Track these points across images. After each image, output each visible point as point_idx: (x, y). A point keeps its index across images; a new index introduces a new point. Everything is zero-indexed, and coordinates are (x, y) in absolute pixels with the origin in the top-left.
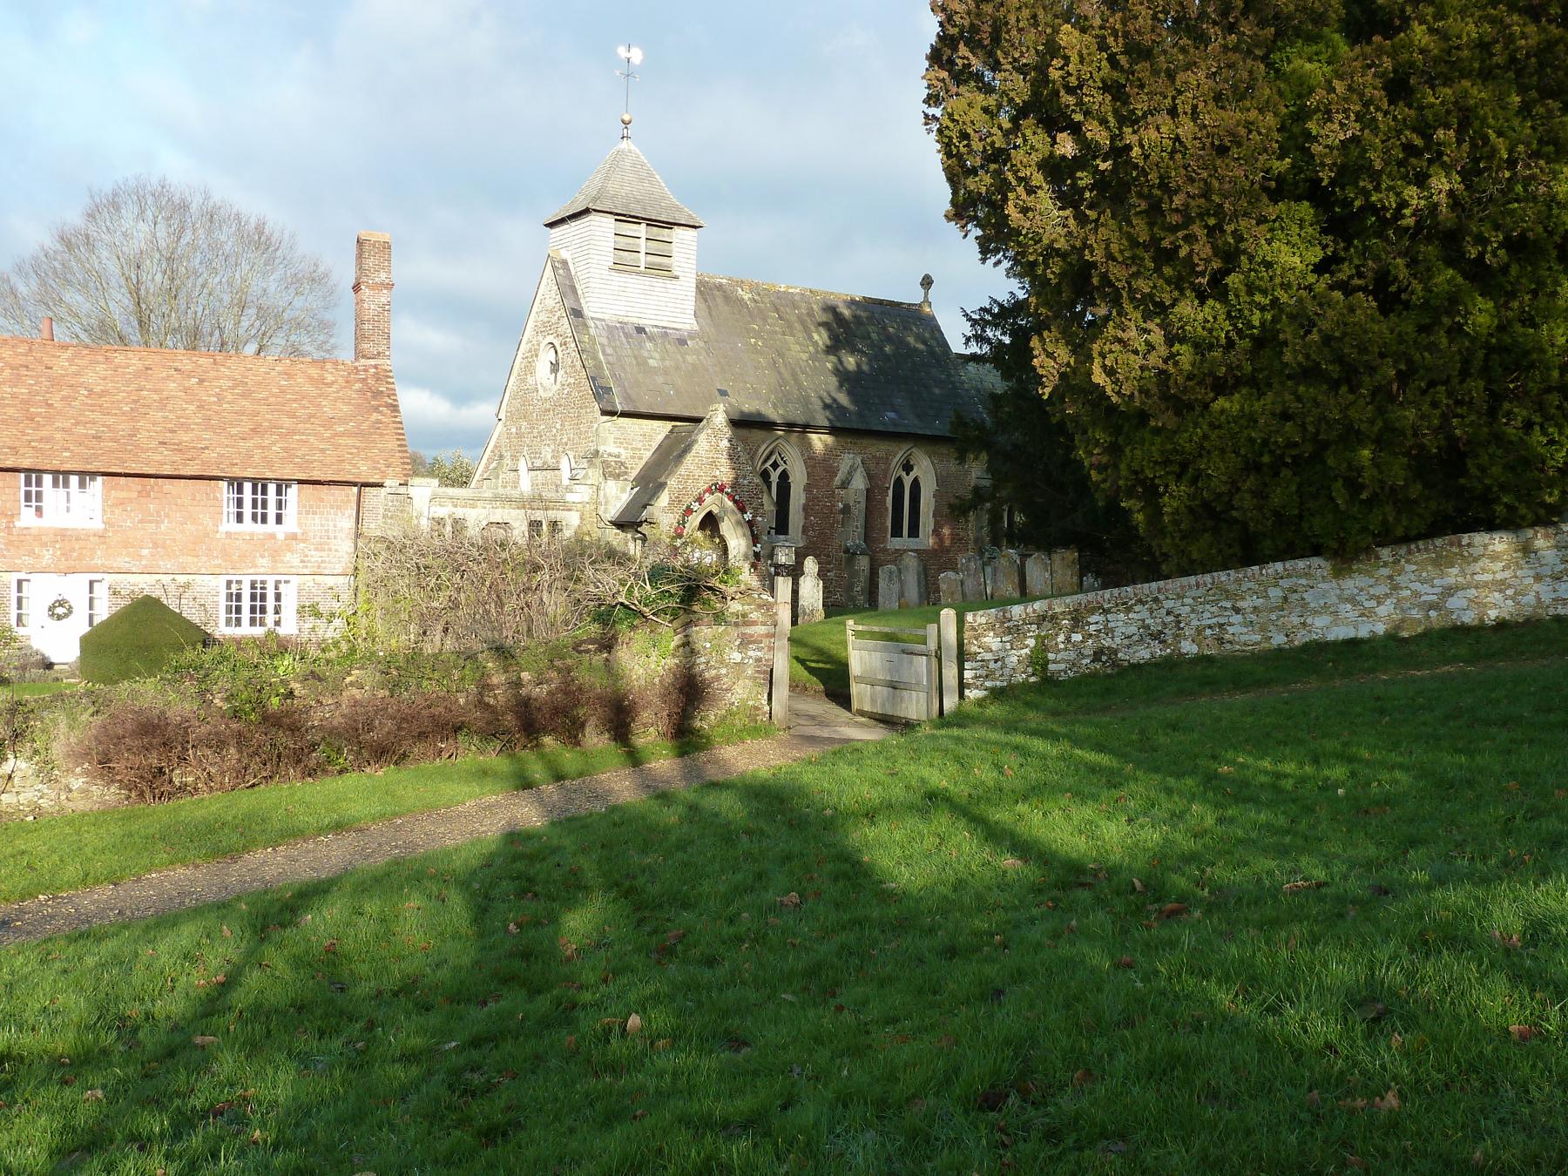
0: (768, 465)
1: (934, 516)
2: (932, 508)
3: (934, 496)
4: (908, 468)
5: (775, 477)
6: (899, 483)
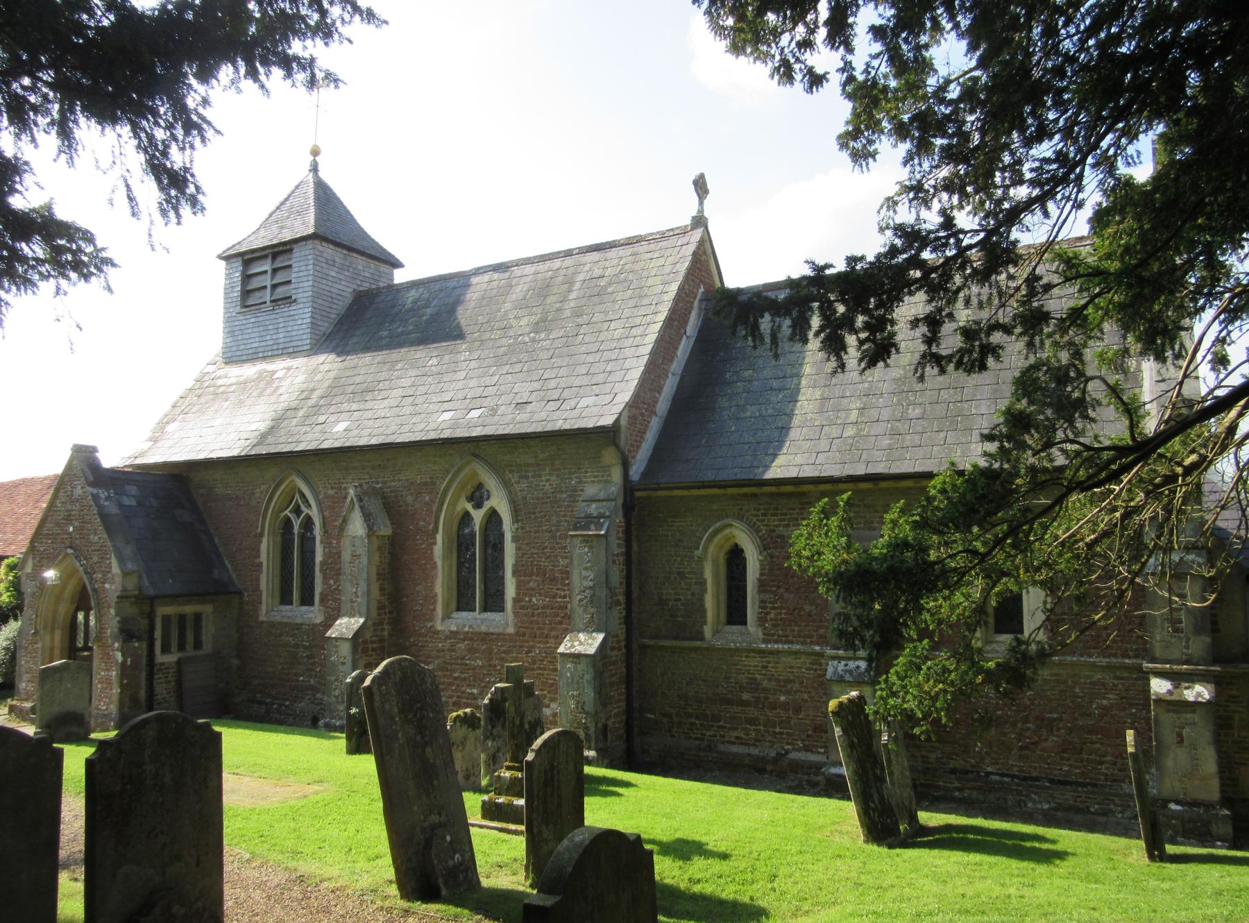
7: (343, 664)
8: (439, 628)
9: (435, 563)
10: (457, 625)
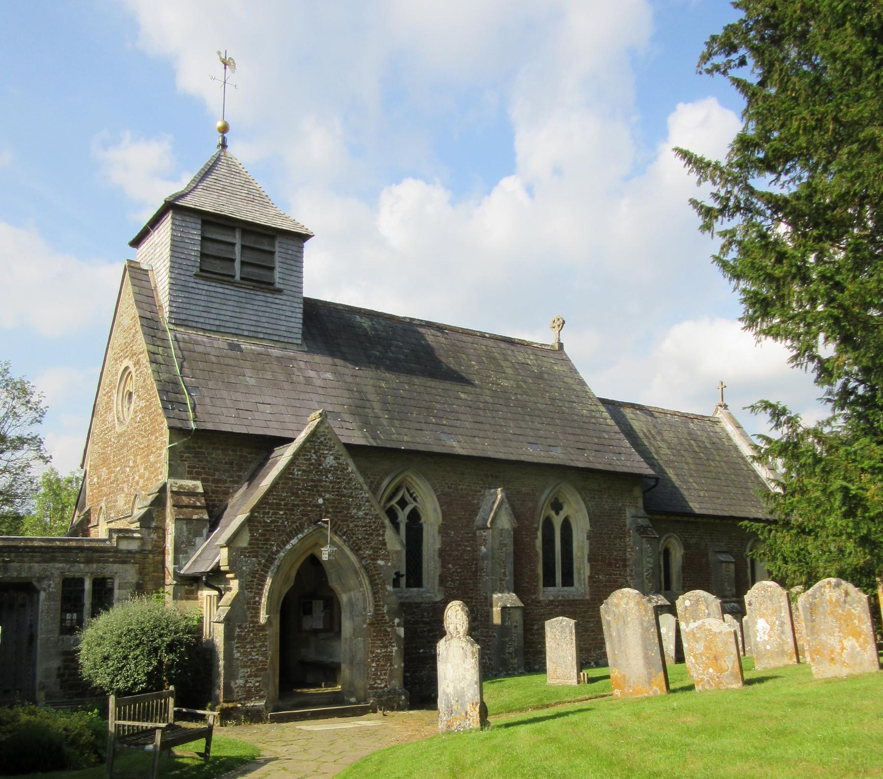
0: (393, 502)
1: (590, 560)
2: (586, 552)
3: (589, 538)
4: (557, 507)
5: (403, 516)
6: (548, 524)
7: (516, 627)
8: (541, 599)
9: (537, 552)
10: (553, 596)
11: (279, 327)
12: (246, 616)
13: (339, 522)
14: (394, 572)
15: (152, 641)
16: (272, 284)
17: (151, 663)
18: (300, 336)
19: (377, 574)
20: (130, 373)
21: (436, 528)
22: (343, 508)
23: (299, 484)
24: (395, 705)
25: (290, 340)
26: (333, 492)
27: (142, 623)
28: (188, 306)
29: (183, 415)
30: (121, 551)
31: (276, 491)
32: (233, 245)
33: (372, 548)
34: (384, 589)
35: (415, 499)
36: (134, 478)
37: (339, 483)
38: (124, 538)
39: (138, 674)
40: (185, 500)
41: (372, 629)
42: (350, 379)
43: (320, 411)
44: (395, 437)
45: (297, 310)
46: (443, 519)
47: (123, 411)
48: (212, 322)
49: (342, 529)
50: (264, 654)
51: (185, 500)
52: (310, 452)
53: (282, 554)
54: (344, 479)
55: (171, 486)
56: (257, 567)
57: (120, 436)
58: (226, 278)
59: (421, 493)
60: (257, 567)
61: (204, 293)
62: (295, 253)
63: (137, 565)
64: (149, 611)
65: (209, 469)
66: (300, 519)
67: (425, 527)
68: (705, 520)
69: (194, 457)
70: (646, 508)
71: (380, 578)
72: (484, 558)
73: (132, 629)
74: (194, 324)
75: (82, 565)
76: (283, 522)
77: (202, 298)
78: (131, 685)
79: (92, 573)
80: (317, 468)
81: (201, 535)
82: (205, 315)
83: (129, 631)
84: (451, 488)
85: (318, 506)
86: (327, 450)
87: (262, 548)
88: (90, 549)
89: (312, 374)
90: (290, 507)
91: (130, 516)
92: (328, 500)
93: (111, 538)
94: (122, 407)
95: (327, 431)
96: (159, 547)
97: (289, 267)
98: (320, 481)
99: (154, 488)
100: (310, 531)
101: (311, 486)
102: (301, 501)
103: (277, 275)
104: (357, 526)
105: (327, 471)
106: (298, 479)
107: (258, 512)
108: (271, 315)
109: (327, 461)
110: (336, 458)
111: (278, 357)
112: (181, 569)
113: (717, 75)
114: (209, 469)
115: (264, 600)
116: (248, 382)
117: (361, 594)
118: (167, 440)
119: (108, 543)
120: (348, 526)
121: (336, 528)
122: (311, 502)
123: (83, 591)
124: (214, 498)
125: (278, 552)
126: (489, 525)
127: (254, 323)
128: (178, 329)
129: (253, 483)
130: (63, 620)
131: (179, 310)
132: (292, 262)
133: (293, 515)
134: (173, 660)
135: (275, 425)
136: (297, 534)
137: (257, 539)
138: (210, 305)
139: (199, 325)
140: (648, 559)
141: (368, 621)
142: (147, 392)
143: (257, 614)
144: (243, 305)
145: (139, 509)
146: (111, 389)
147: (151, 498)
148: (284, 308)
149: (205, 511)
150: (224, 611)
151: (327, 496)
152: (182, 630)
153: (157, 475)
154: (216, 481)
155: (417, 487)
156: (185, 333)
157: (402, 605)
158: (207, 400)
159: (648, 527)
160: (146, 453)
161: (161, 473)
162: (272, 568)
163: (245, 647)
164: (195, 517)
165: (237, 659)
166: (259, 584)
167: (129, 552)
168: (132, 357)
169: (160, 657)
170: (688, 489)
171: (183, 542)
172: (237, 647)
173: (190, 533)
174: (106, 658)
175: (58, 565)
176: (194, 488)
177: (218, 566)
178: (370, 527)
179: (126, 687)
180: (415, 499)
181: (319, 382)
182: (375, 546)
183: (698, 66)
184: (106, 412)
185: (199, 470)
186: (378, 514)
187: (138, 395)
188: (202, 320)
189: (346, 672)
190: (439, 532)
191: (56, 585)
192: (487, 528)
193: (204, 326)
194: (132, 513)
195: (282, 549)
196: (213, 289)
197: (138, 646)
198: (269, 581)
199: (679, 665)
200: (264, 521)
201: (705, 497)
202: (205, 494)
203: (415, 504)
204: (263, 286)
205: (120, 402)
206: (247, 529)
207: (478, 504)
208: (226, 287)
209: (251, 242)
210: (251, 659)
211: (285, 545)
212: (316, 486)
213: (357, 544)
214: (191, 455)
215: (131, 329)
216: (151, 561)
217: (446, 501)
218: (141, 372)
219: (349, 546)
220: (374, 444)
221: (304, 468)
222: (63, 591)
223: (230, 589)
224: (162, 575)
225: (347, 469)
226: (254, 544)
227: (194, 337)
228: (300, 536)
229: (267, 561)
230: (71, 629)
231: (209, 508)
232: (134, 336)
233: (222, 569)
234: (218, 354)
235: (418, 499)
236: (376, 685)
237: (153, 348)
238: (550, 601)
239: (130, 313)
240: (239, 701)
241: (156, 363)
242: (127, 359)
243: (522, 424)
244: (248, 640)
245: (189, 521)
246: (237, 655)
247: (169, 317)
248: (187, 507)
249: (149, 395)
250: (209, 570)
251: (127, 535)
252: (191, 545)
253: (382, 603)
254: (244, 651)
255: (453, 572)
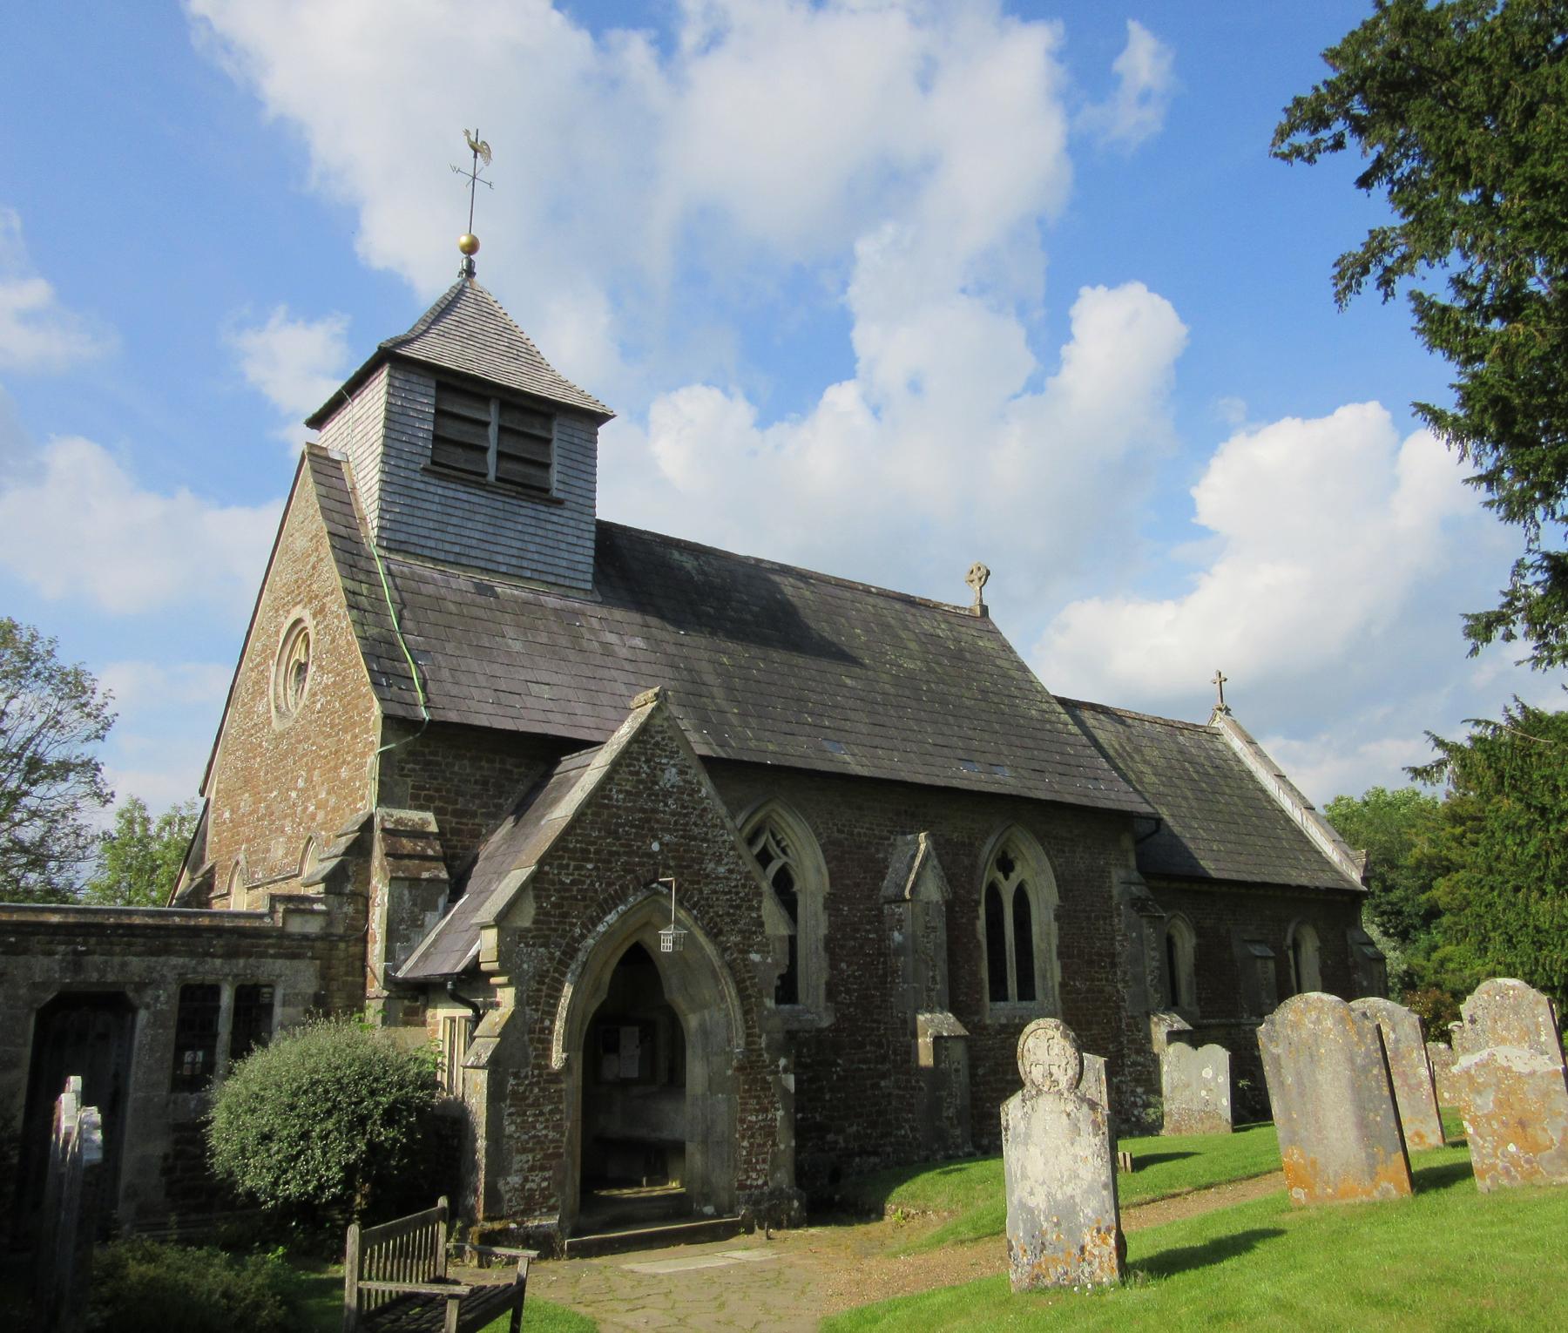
4: (1006, 866)
9: (978, 941)
11: (557, 561)
12: (526, 1056)
13: (686, 885)
14: (777, 974)
15: (356, 1104)
16: (547, 491)
17: (354, 1147)
18: (589, 577)
19: (749, 978)
20: (305, 628)
21: (820, 900)
22: (693, 860)
23: (620, 817)
24: (784, 1217)
25: (574, 584)
26: (677, 830)
27: (337, 1068)
28: (410, 520)
29: (407, 696)
30: (290, 936)
31: (581, 828)
32: (486, 424)
33: (740, 931)
34: (761, 1004)
35: (784, 851)
36: (306, 808)
37: (686, 815)
38: (297, 911)
39: (329, 1168)
40: (407, 845)
41: (742, 1078)
42: (672, 649)
43: (656, 690)
44: (753, 744)
45: (587, 535)
46: (832, 885)
47: (285, 695)
48: (447, 547)
49: (692, 897)
50: (557, 1127)
51: (407, 845)
52: (639, 760)
53: (591, 941)
54: (695, 809)
55: (382, 819)
56: (548, 965)
57: (282, 736)
58: (473, 478)
59: (794, 838)
60: (548, 965)
61: (437, 499)
62: (583, 443)
63: (318, 962)
64: (348, 1045)
65: (448, 791)
66: (620, 877)
67: (800, 898)
68: (1224, 889)
69: (422, 770)
70: (1140, 868)
71: (753, 985)
72: (900, 950)
73: (318, 1081)
74: (419, 551)
75: (218, 962)
76: (592, 884)
77: (434, 507)
78: (315, 1188)
79: (236, 976)
80: (650, 789)
81: (435, 908)
82: (438, 535)
83: (314, 1083)
84: (843, 832)
85: (652, 855)
86: (666, 757)
87: (555, 930)
88: (234, 931)
89: (611, 638)
90: (604, 855)
91: (296, 876)
92: (667, 845)
93: (272, 911)
94: (285, 689)
95: (666, 724)
96: (357, 929)
97: (575, 465)
98: (654, 811)
99: (349, 823)
100: (639, 899)
101: (640, 820)
102: (622, 845)
103: (555, 476)
104: (715, 892)
105: (667, 794)
106: (618, 808)
107: (551, 865)
108: (544, 541)
109: (667, 775)
110: (681, 772)
111: (556, 609)
112: (397, 969)
113: (1297, 161)
114: (448, 791)
115: (559, 1026)
116: (509, 647)
117: (723, 1014)
118: (376, 737)
119: (267, 920)
120: (701, 892)
121: (680, 895)
122: (639, 848)
123: (218, 1008)
124: (454, 843)
125: (583, 937)
126: (908, 896)
127: (515, 552)
128: (392, 556)
129: (525, 817)
130: (178, 1061)
131: (395, 526)
132: (580, 458)
133: (610, 870)
134: (395, 1140)
135: (558, 718)
136: (616, 906)
137: (547, 914)
138: (445, 519)
139: (427, 552)
140: (1153, 954)
141: (735, 1063)
142: (338, 659)
143: (546, 1053)
144: (499, 522)
145: (322, 860)
146: (265, 659)
147: (344, 843)
148: (565, 530)
149: (442, 865)
150: (485, 1046)
151: (667, 838)
152: (411, 1082)
153: (355, 802)
154: (456, 813)
155: (788, 830)
156: (403, 564)
157: (791, 1035)
158: (445, 674)
159: (1148, 899)
160: (332, 764)
161: (363, 798)
162: (573, 966)
163: (525, 1114)
164: (425, 875)
165: (510, 1137)
166: (549, 996)
167: (305, 937)
168: (310, 602)
169: (371, 1133)
170: (1194, 839)
171: (402, 920)
172: (510, 1115)
173: (415, 904)
174: (266, 1138)
175: (174, 960)
176: (423, 825)
177: (476, 962)
178: (737, 893)
179: (302, 1195)
180: (784, 851)
181: (623, 652)
182: (745, 928)
183: (1273, 145)
184: (253, 699)
185: (431, 793)
186: (749, 872)
187: (320, 667)
188: (431, 543)
189: (695, 1157)
190: (826, 907)
191: (169, 996)
192: (905, 900)
193: (434, 555)
194: (301, 870)
195: (589, 931)
196: (451, 493)
197: (329, 1113)
198: (568, 990)
199: (1257, 1134)
200: (560, 880)
201: (1219, 851)
202: (440, 835)
203: (784, 859)
204: (534, 493)
205: (281, 681)
206: (531, 893)
207: (885, 859)
208: (473, 491)
209: (513, 420)
210: (534, 1137)
211: (595, 925)
212: (648, 820)
213: (716, 924)
214: (417, 767)
215: (310, 555)
216: (342, 955)
217: (836, 854)
218: (326, 627)
219: (702, 928)
220: (724, 756)
221: (628, 788)
222: (181, 1009)
223: (497, 1005)
224: (360, 980)
225: (699, 791)
226: (542, 922)
227: (417, 569)
228: (621, 908)
229: (564, 953)
230: (196, 1081)
231: (448, 859)
232: (314, 568)
233: (484, 967)
234: (459, 600)
235: (789, 851)
236: (749, 1182)
237: (351, 585)
238: (1002, 1026)
239: (311, 523)
240: (513, 1217)
241: (358, 609)
242: (299, 607)
243: (945, 730)
244: (530, 1101)
245: (414, 882)
246: (510, 1129)
247: (378, 536)
248: (410, 857)
249: (343, 663)
250: (459, 968)
251: (302, 907)
252: (418, 926)
253: (757, 1030)
254: (523, 1122)
255: (848, 976)
